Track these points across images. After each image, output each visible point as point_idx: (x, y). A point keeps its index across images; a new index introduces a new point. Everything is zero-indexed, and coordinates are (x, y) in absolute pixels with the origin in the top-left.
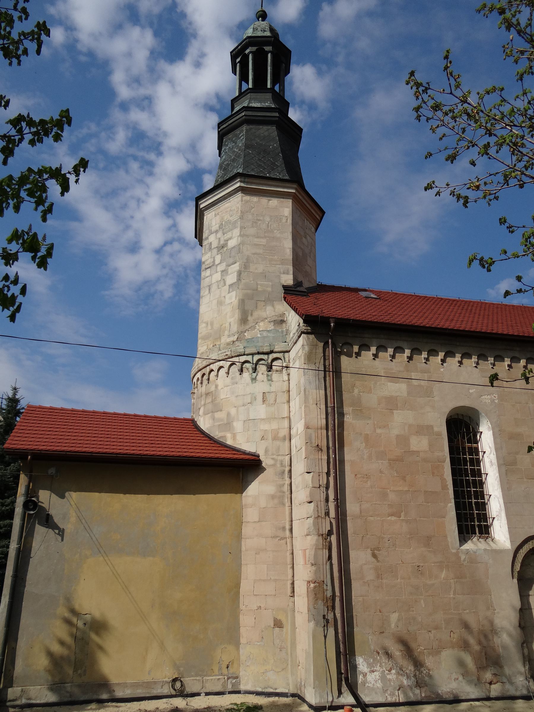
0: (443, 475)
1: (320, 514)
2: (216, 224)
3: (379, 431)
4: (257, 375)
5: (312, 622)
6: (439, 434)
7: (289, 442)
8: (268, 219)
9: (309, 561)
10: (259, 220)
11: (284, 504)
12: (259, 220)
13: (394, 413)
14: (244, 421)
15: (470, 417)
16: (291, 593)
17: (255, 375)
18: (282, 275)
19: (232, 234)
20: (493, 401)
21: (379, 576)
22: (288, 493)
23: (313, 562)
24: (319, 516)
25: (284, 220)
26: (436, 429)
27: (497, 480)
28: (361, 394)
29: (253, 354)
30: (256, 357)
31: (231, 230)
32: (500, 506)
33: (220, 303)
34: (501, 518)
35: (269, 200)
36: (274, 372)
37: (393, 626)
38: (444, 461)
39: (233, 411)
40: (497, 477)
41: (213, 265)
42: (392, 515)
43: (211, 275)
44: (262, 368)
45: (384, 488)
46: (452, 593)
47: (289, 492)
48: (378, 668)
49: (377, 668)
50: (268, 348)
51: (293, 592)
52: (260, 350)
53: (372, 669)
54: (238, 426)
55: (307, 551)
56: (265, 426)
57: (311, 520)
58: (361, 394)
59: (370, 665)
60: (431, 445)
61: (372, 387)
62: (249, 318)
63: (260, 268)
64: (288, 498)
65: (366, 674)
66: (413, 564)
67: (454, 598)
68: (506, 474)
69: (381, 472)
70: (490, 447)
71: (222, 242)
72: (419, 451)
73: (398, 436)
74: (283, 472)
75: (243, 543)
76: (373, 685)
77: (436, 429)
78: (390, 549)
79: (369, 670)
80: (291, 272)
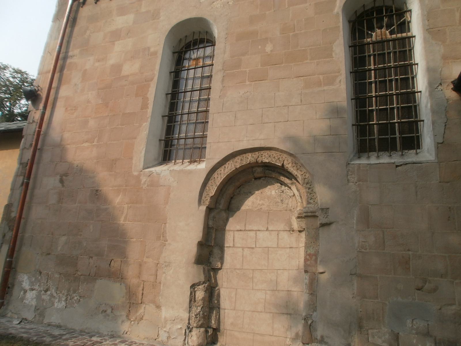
3: (97, 64)
15: (207, 32)
42: (87, 141)
48: (37, 287)
53: (33, 287)
59: (32, 283)
65: (27, 291)
68: (223, 81)
79: (29, 287)
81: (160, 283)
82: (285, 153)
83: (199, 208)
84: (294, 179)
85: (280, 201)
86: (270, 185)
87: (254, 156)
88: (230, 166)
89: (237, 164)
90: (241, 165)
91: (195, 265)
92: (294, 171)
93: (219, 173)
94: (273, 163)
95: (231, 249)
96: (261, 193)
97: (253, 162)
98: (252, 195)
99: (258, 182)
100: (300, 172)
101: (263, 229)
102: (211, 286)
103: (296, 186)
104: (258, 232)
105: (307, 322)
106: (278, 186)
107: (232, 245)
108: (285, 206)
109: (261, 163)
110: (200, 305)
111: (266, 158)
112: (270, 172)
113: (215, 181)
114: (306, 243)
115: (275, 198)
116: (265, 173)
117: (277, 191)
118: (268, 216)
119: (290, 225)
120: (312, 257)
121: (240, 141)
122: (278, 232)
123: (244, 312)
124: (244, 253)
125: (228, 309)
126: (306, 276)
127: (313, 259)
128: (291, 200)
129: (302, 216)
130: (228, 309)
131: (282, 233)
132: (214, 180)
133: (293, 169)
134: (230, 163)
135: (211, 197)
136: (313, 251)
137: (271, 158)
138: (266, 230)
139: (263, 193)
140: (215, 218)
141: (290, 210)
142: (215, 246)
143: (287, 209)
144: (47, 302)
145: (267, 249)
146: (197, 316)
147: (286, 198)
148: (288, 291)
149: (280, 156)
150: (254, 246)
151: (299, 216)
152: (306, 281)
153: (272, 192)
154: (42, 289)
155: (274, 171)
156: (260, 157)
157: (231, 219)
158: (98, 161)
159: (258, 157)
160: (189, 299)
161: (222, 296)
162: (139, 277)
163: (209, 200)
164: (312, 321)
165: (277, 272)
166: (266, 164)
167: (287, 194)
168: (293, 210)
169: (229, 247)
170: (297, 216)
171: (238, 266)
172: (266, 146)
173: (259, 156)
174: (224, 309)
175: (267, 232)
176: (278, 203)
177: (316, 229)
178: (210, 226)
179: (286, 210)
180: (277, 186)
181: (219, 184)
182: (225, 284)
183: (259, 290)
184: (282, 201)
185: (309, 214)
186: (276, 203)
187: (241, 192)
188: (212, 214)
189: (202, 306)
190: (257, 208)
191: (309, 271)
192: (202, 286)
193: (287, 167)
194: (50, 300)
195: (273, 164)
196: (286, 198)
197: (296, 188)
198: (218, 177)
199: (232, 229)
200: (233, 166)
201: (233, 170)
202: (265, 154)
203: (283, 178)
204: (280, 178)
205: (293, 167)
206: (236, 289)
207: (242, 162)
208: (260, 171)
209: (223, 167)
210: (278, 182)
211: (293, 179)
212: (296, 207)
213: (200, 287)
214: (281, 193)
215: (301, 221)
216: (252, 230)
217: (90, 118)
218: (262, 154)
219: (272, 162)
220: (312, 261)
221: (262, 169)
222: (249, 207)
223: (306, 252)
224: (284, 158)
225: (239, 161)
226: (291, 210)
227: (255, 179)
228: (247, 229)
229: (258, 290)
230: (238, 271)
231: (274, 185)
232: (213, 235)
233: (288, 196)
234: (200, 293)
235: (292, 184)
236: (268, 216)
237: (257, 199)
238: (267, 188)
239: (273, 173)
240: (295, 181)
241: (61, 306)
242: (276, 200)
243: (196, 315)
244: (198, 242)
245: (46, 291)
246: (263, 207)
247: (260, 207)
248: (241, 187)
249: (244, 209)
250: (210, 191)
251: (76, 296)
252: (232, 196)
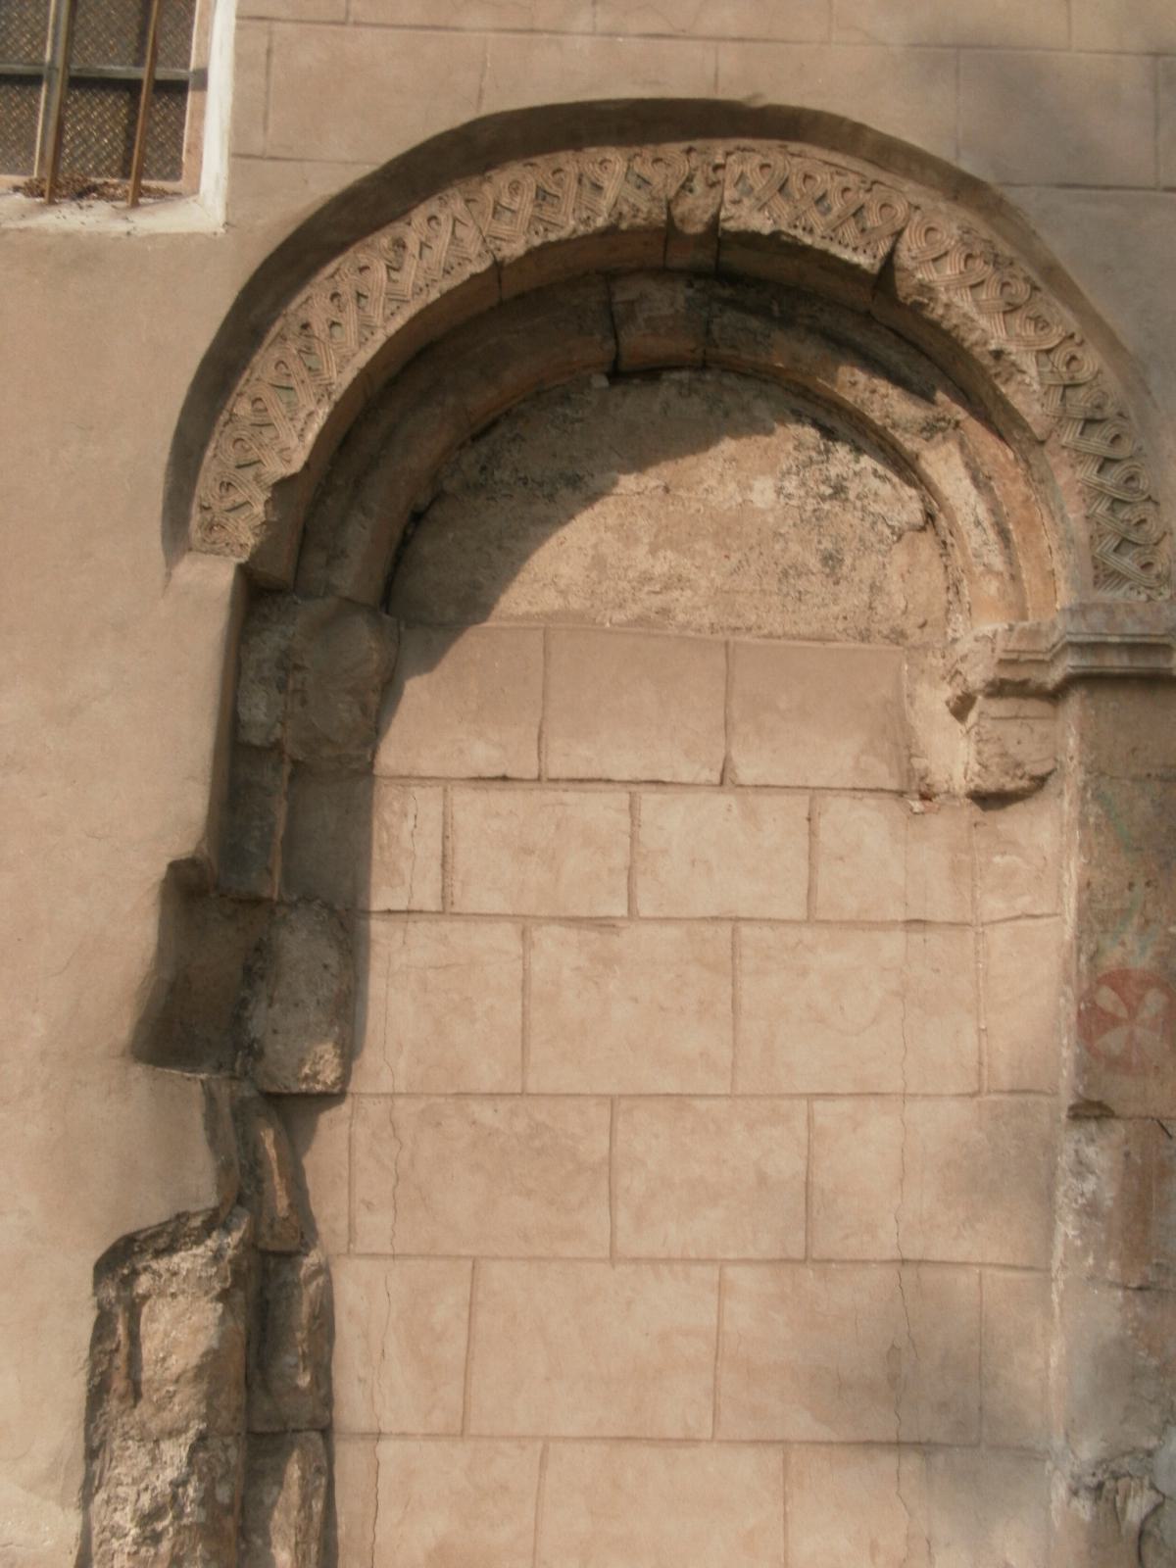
82: (907, 173)
83: (169, 575)
84: (947, 392)
85: (814, 563)
86: (736, 433)
87: (647, 171)
88: (447, 238)
89: (503, 228)
90: (537, 241)
91: (138, 1070)
92: (983, 322)
93: (346, 289)
94: (808, 240)
95: (420, 930)
96: (667, 490)
97: (639, 221)
98: (591, 499)
99: (638, 404)
100: (1030, 331)
101: (685, 778)
102: (261, 1245)
103: (962, 446)
104: (650, 799)
106: (796, 448)
107: (432, 904)
108: (853, 599)
109: (700, 240)
110: (181, 1424)
111: (747, 202)
112: (755, 323)
113: (309, 351)
114: (1089, 884)
115: (777, 535)
116: (708, 332)
117: (791, 485)
118: (729, 679)
119: (903, 745)
120: (1140, 998)
121: (532, 31)
122: (812, 799)
123: (545, 1449)
124: (538, 967)
125: (403, 1435)
126: (1090, 1152)
127: (1145, 1014)
128: (900, 557)
129: (1024, 683)
130: (403, 1435)
132: (301, 343)
133: (977, 303)
134: (442, 217)
135: (283, 485)
136: (1143, 949)
137: (788, 197)
138: (715, 778)
139: (682, 493)
140: (298, 668)
141: (898, 636)
142: (293, 906)
143: (874, 627)
145: (725, 931)
146: (160, 1526)
147: (861, 540)
148: (904, 1261)
149: (869, 190)
150: (621, 910)
151: (1006, 675)
152: (1090, 1185)
153: (750, 488)
155: (786, 322)
156: (698, 186)
157: (416, 690)
159: (686, 187)
160: (83, 1377)
161: (346, 1329)
163: (259, 509)
164: (1158, 1499)
165: (810, 1119)
166: (734, 258)
167: (875, 508)
168: (916, 637)
169: (409, 912)
170: (991, 676)
171: (488, 1073)
172: (756, 96)
173: (690, 179)
174: (364, 1435)
175: (725, 800)
176: (799, 575)
177: (1162, 779)
178: (256, 737)
179: (865, 636)
180: (790, 446)
181: (349, 375)
182: (376, 1227)
183: (668, 1261)
184: (831, 560)
185: (1116, 662)
186: (785, 574)
187: (497, 475)
188: (271, 642)
189: (197, 1426)
190: (634, 610)
191: (1117, 1109)
192: (200, 1250)
193: (925, 288)
195: (806, 250)
196: (861, 540)
197: (967, 465)
198: (333, 324)
199: (427, 766)
200: (473, 248)
201: (474, 277)
202: (747, 168)
203: (861, 377)
204: (834, 381)
205: (973, 287)
206: (475, 1260)
207: (547, 213)
208: (671, 311)
209: (383, 240)
210: (799, 417)
211: (940, 396)
212: (940, 614)
213: (189, 1260)
214: (823, 498)
215: (1016, 717)
216: (600, 780)
218: (717, 168)
219: (799, 233)
220: (1139, 1032)
221: (687, 300)
222: (563, 593)
223: (1092, 958)
224: (900, 209)
225: (524, 204)
226: (903, 634)
227: (617, 374)
228: (557, 768)
229: (653, 1261)
230: (485, 1113)
231: (769, 432)
232: (281, 812)
233: (881, 527)
234: (177, 1320)
235: (930, 429)
236: (729, 679)
237: (629, 539)
238: (712, 452)
239: (777, 336)
240: (959, 413)
242: (785, 550)
243: (146, 1519)
244: (174, 867)
246: (681, 599)
247: (657, 601)
248: (496, 433)
249: (524, 608)
250: (268, 433)
252: (423, 499)
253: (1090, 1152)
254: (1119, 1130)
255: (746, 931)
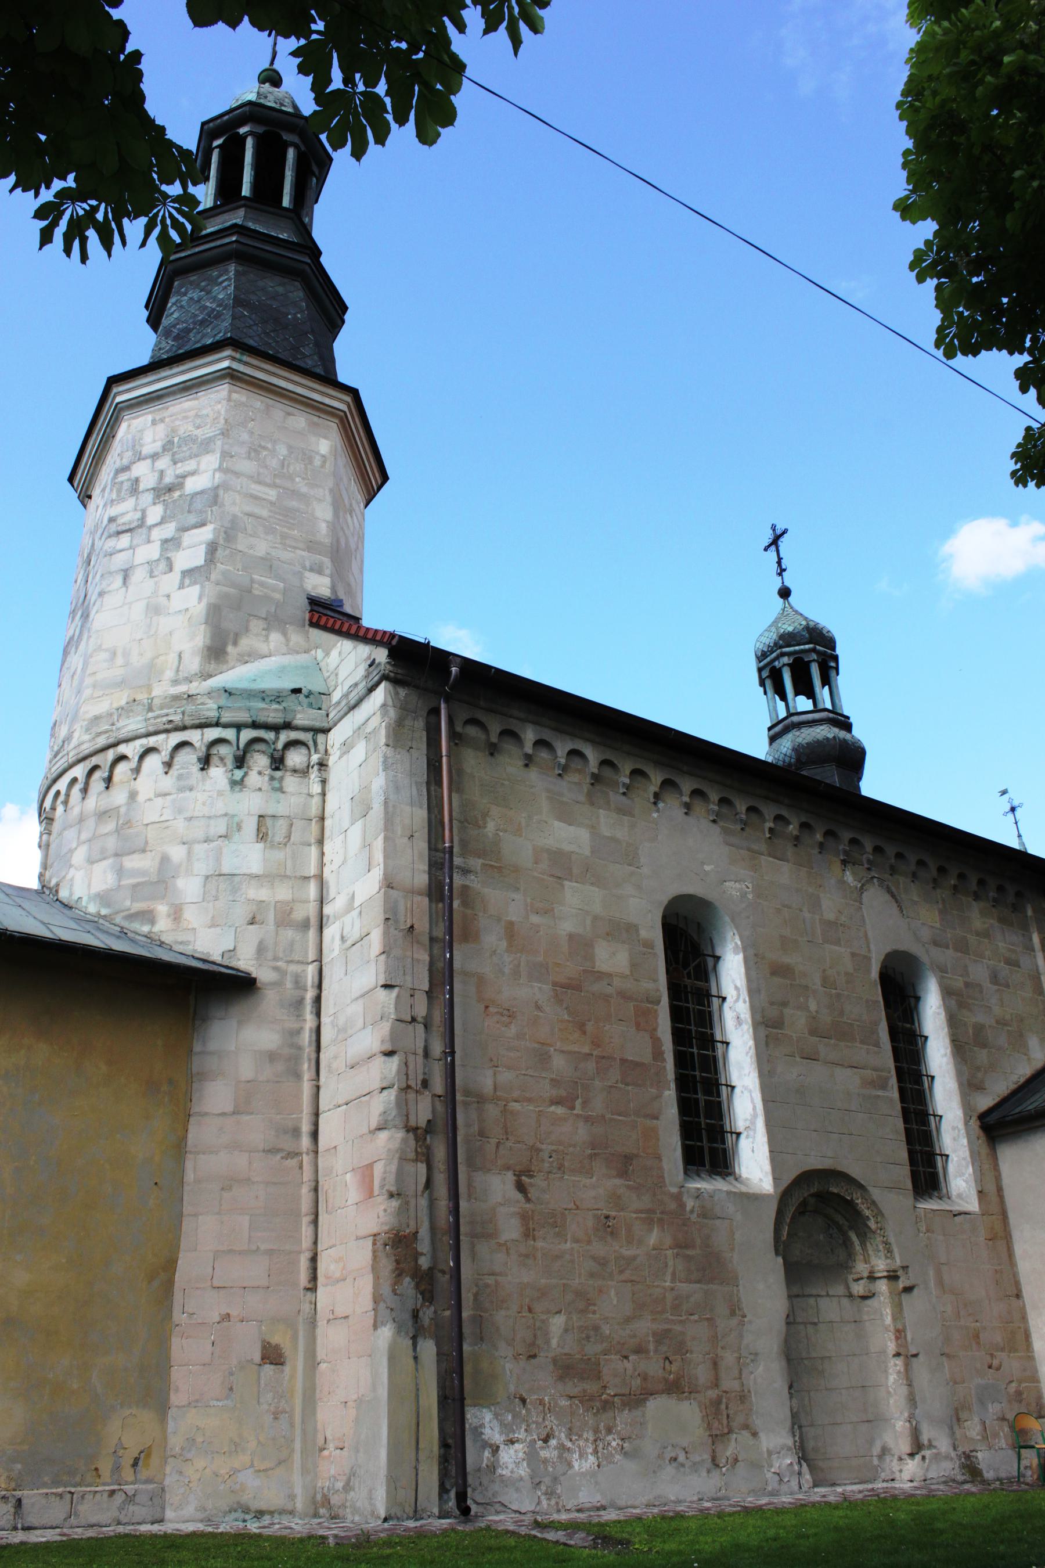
0: (655, 1030)
1: (412, 1083)
2: (154, 441)
3: (535, 919)
4: (246, 774)
5: (388, 1326)
6: (649, 945)
7: (319, 934)
8: (282, 450)
9: (382, 1186)
10: (265, 448)
11: (298, 1076)
12: (265, 448)
13: (566, 887)
14: (207, 877)
16: (309, 1282)
17: (238, 774)
18: (307, 574)
19: (198, 464)
20: (744, 895)
21: (528, 1234)
22: (309, 1050)
23: (393, 1189)
24: (408, 1087)
25: (317, 462)
26: (644, 934)
27: (750, 1054)
28: (501, 834)
29: (239, 727)
30: (247, 735)
31: (196, 456)
32: (754, 1108)
33: (154, 610)
34: (755, 1133)
35: (289, 414)
36: (288, 773)
37: (554, 1342)
38: (658, 1002)
39: (177, 853)
40: (750, 1048)
41: (140, 526)
43: (132, 547)
44: (260, 761)
45: (543, 1044)
46: (668, 1278)
47: (314, 1048)
48: (521, 1435)
49: (519, 1434)
50: (280, 715)
51: (314, 1278)
52: (259, 718)
53: (511, 1436)
54: (189, 887)
55: (378, 1169)
56: (263, 894)
57: (391, 1095)
58: (501, 834)
59: (506, 1428)
60: (634, 966)
61: (523, 824)
62: (230, 649)
63: (261, 547)
64: (310, 1060)
65: (498, 1447)
66: (596, 1212)
67: (672, 1289)
69: (538, 1007)
70: (737, 988)
71: (168, 479)
72: (611, 975)
73: (571, 937)
74: (300, 1002)
75: (189, 1165)
76: (512, 1472)
77: (644, 934)
78: (553, 1176)
80: (328, 572)
81: (749, 1391)
104: (819, 1299)
105: (912, 1425)
126: (897, 1362)
131: (842, 1298)
144: (553, 1463)
152: (898, 1368)
154: (535, 1437)
158: (595, 1154)
162: (717, 1385)
175: (828, 1298)
184: (832, 1250)
193: (857, 1204)
194: (560, 1457)
217: (552, 1049)
230: (806, 1362)
241: (588, 1466)
245: (546, 1440)
251: (614, 1440)
253: (897, 1362)
254: (902, 1358)
255: (834, 1324)
